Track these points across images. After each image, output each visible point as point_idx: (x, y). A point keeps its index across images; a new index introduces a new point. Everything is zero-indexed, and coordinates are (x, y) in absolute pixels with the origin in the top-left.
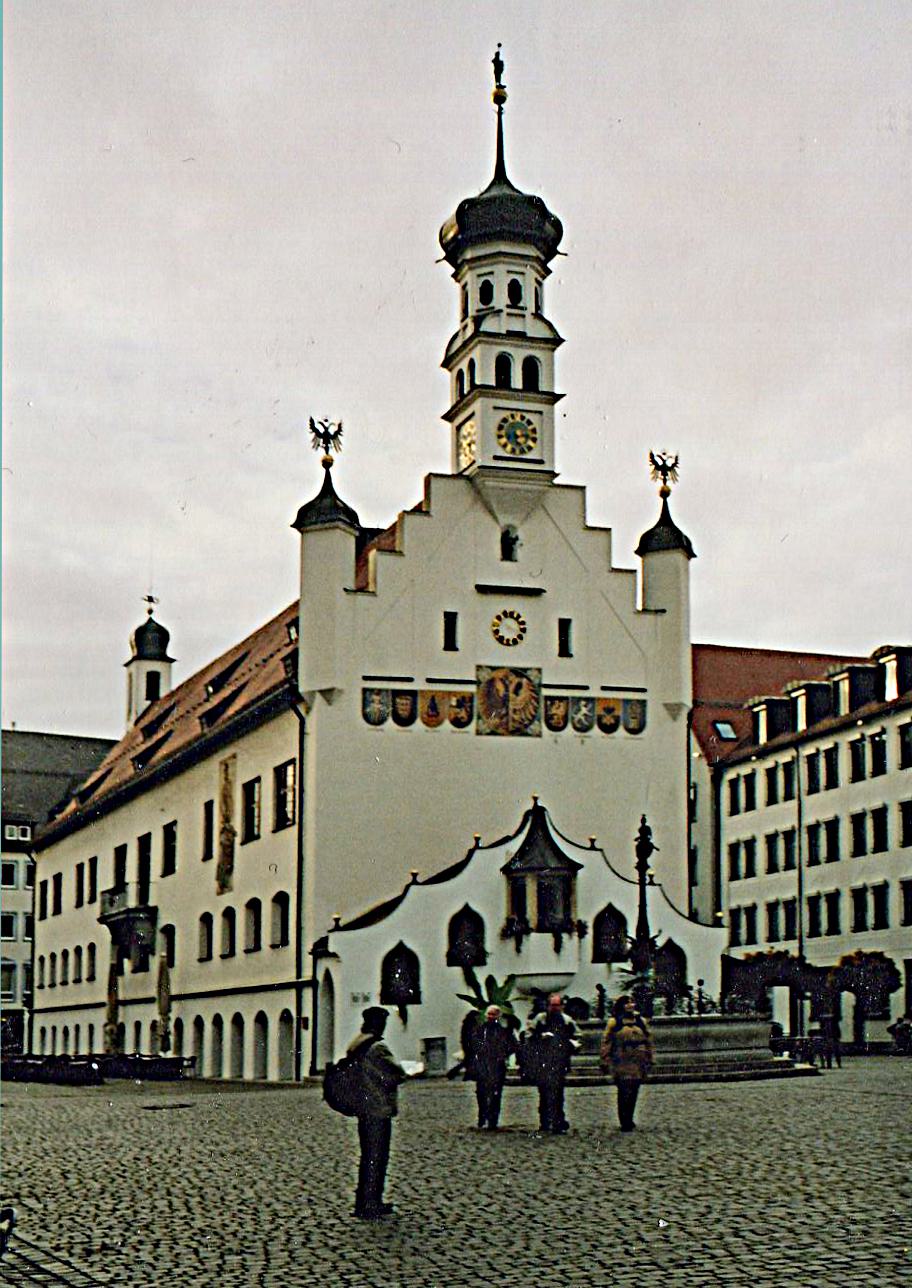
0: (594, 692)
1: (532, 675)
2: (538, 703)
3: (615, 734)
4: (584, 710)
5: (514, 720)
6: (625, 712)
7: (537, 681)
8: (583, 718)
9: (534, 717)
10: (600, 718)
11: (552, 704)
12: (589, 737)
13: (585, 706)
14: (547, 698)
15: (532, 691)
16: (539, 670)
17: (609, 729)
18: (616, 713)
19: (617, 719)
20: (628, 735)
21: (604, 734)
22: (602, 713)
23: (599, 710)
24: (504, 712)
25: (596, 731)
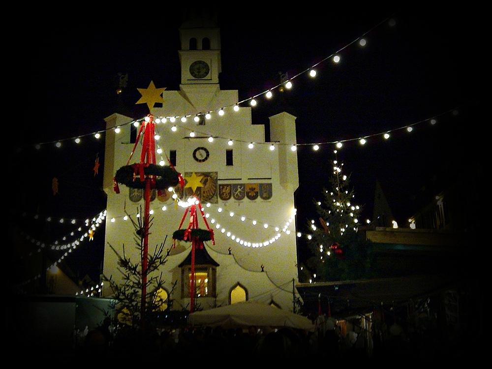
0: (244, 181)
1: (213, 175)
2: (216, 188)
3: (256, 200)
4: (239, 190)
5: (204, 196)
6: (261, 191)
7: (216, 178)
8: (239, 194)
9: (214, 194)
10: (248, 193)
11: (222, 189)
12: (242, 202)
13: (240, 188)
14: (220, 185)
15: (212, 182)
16: (217, 173)
17: (253, 198)
18: (256, 190)
19: (257, 193)
20: (262, 200)
21: (250, 201)
22: (249, 191)
23: (247, 190)
24: (199, 193)
25: (246, 199)
